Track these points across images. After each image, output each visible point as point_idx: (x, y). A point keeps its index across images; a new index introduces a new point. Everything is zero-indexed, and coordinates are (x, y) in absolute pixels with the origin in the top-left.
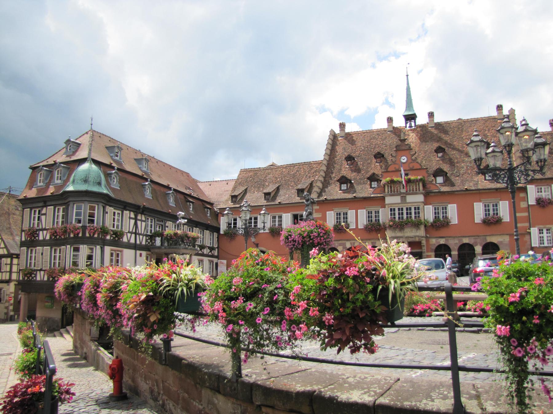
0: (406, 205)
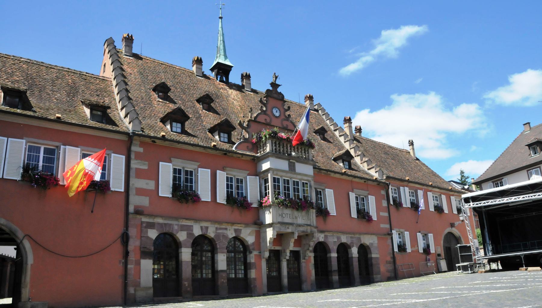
0: (295, 176)
